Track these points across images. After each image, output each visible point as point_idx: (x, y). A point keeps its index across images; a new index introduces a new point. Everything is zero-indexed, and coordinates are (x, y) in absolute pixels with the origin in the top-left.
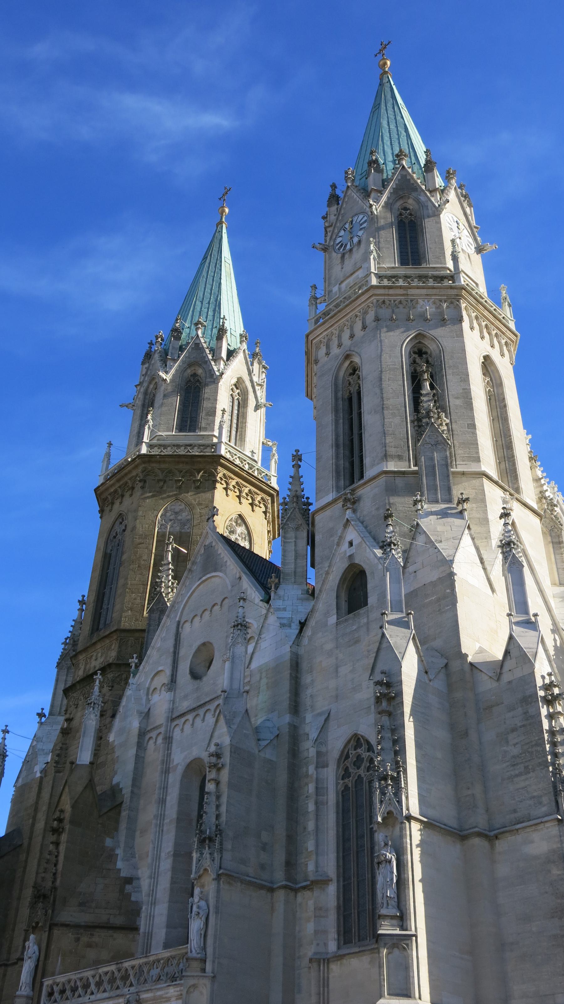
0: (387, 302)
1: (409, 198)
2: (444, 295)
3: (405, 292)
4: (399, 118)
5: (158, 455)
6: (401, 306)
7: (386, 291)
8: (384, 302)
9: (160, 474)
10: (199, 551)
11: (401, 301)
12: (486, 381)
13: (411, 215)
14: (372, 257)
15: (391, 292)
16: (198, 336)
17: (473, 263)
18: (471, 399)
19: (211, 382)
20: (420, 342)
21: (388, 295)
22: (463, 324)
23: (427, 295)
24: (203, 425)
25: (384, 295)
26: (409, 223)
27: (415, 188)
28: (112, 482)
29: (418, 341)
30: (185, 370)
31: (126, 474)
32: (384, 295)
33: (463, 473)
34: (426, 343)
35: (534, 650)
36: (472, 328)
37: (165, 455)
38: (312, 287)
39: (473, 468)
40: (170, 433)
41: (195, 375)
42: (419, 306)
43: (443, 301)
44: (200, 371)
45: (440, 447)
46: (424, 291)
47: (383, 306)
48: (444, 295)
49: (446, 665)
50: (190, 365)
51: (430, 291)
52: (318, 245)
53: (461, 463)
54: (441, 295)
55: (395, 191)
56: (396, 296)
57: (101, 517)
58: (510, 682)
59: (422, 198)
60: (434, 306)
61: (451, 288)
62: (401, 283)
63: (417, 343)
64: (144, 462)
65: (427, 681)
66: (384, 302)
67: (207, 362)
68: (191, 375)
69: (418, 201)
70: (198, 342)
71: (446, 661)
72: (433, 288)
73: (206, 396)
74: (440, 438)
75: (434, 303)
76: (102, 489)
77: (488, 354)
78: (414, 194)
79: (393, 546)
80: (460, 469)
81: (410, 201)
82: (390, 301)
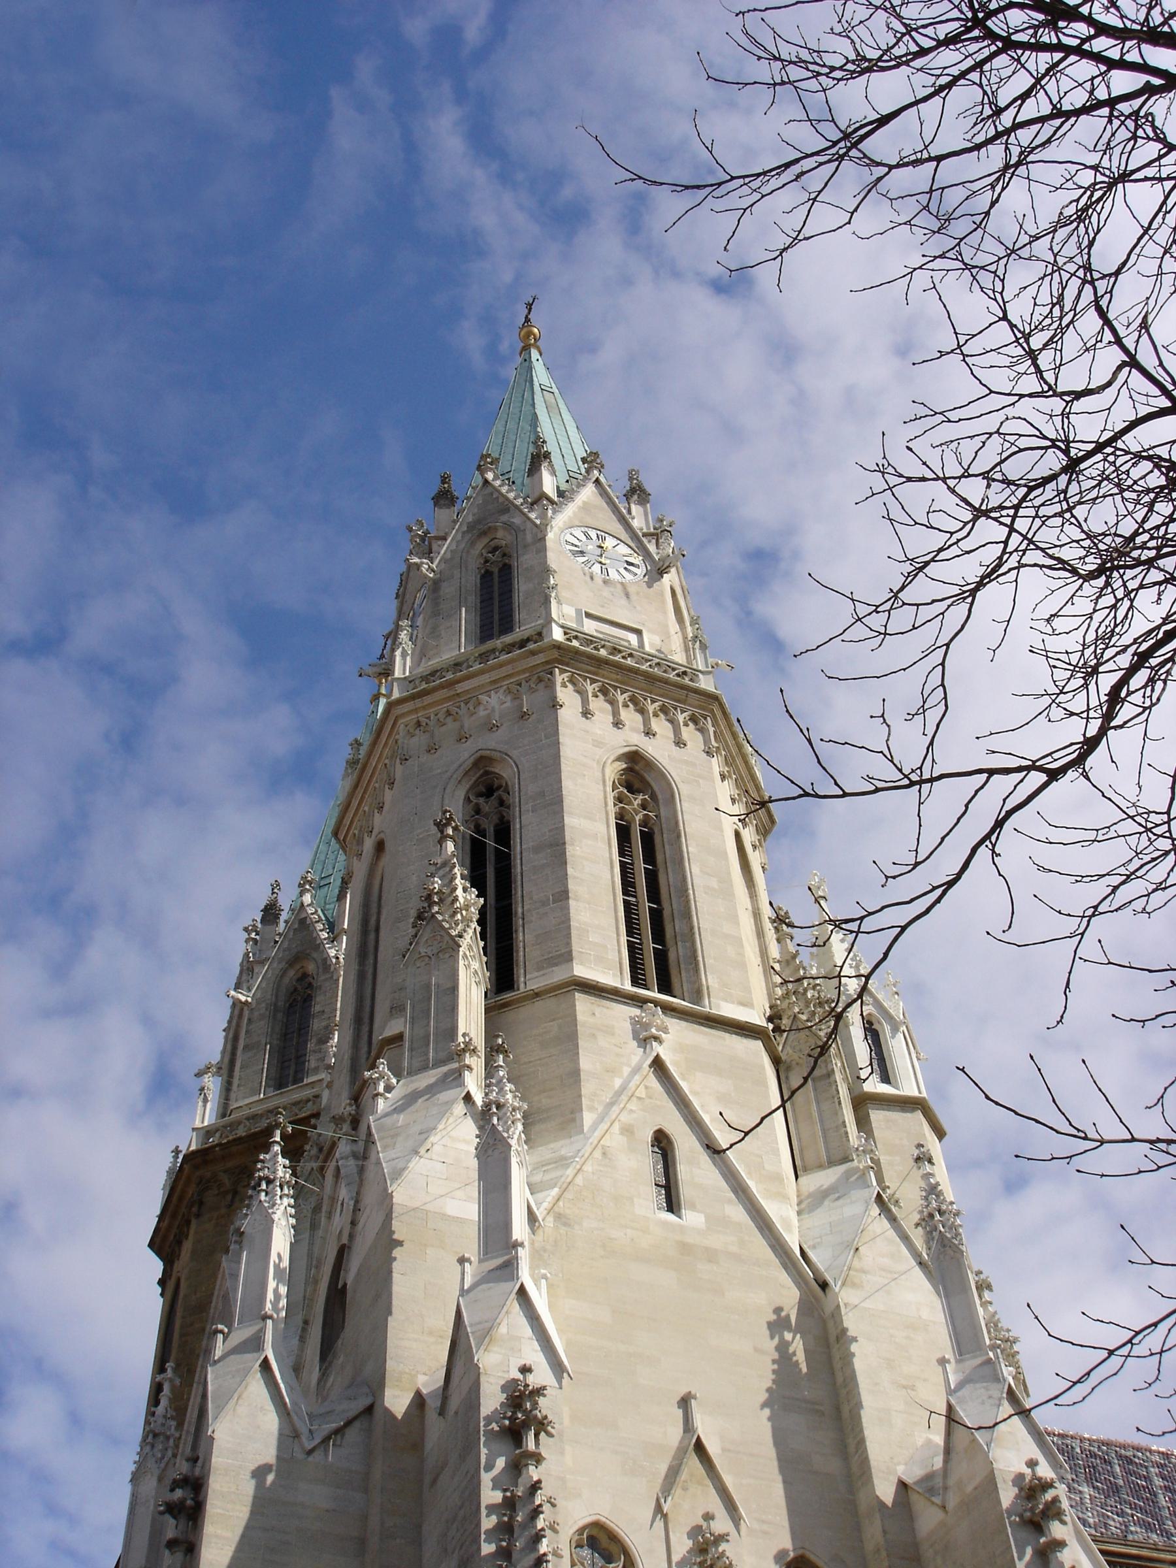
0: (423, 721)
1: (496, 529)
2: (524, 671)
3: (452, 693)
4: (526, 408)
5: (217, 1145)
6: (449, 719)
7: (418, 703)
8: (418, 724)
9: (226, 1181)
10: (216, 1308)
12: (638, 801)
13: (504, 555)
14: (398, 653)
15: (428, 700)
16: (302, 904)
18: (564, 843)
19: (326, 980)
20: (487, 773)
21: (424, 708)
22: (563, 714)
23: (494, 682)
24: (313, 1064)
25: (416, 710)
26: (500, 570)
27: (507, 507)
28: (166, 1222)
30: (284, 972)
31: (181, 1199)
32: (416, 710)
33: (537, 995)
34: (497, 771)
35: (489, 1324)
36: (586, 713)
37: (228, 1142)
38: (351, 745)
39: (558, 975)
40: (256, 1098)
41: (305, 976)
42: (481, 708)
43: (524, 683)
44: (311, 968)
45: (447, 955)
46: (485, 679)
47: (417, 732)
48: (524, 671)
49: (369, 1410)
50: (291, 963)
51: (495, 675)
52: (370, 670)
53: (536, 974)
54: (518, 673)
55: (471, 527)
57: (162, 1295)
58: (456, 1413)
59: (517, 520)
60: (509, 698)
61: (533, 653)
62: (449, 676)
63: (481, 776)
64: (196, 1167)
65: (300, 1455)
66: (418, 724)
67: (318, 946)
68: (298, 980)
69: (509, 526)
70: (303, 916)
71: (367, 1402)
72: (501, 666)
73: (318, 1008)
74: (447, 938)
75: (509, 691)
76: (158, 1240)
77: (634, 748)
78: (504, 518)
79: (264, 1186)
80: (533, 985)
81: (500, 534)
82: (429, 718)
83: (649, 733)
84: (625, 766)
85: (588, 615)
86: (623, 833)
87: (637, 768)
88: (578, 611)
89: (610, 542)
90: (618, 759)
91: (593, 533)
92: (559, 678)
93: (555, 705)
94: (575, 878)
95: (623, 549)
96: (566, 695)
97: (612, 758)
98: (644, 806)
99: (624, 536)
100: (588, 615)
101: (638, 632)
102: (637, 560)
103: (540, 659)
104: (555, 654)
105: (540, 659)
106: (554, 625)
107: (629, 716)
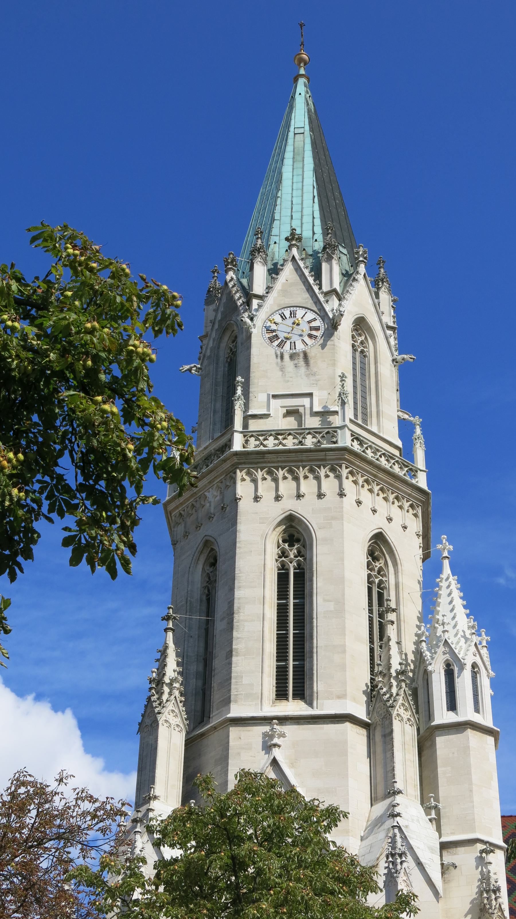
0: (182, 512)
11: (193, 505)
17: (311, 362)
18: (233, 613)
20: (212, 549)
21: (182, 504)
29: (209, 549)
56: (188, 501)
83: (299, 496)
84: (284, 527)
85: (275, 396)
86: (282, 579)
87: (293, 524)
88: (268, 395)
89: (300, 313)
90: (279, 524)
91: (287, 313)
92: (239, 474)
93: (236, 500)
94: (238, 638)
95: (310, 316)
96: (243, 488)
97: (272, 528)
98: (299, 554)
99: (310, 303)
100: (275, 396)
101: (310, 395)
102: (318, 323)
103: (227, 465)
104: (235, 460)
105: (227, 465)
106: (236, 434)
107: (287, 487)
